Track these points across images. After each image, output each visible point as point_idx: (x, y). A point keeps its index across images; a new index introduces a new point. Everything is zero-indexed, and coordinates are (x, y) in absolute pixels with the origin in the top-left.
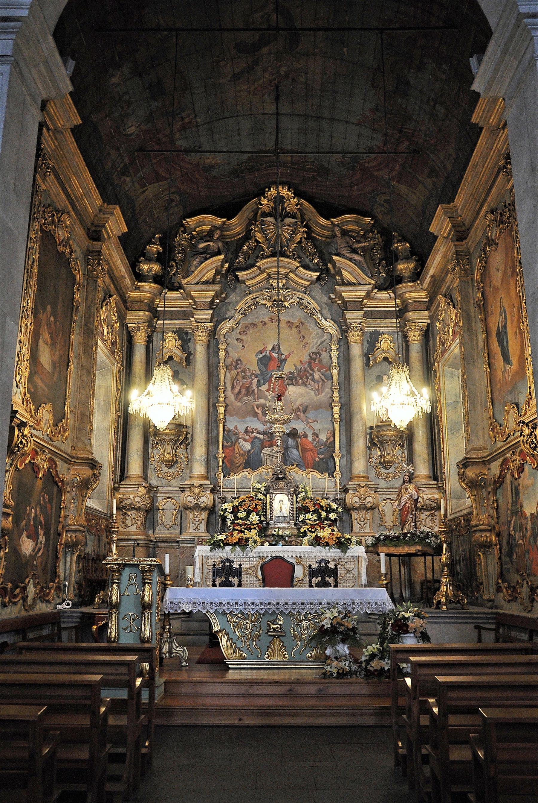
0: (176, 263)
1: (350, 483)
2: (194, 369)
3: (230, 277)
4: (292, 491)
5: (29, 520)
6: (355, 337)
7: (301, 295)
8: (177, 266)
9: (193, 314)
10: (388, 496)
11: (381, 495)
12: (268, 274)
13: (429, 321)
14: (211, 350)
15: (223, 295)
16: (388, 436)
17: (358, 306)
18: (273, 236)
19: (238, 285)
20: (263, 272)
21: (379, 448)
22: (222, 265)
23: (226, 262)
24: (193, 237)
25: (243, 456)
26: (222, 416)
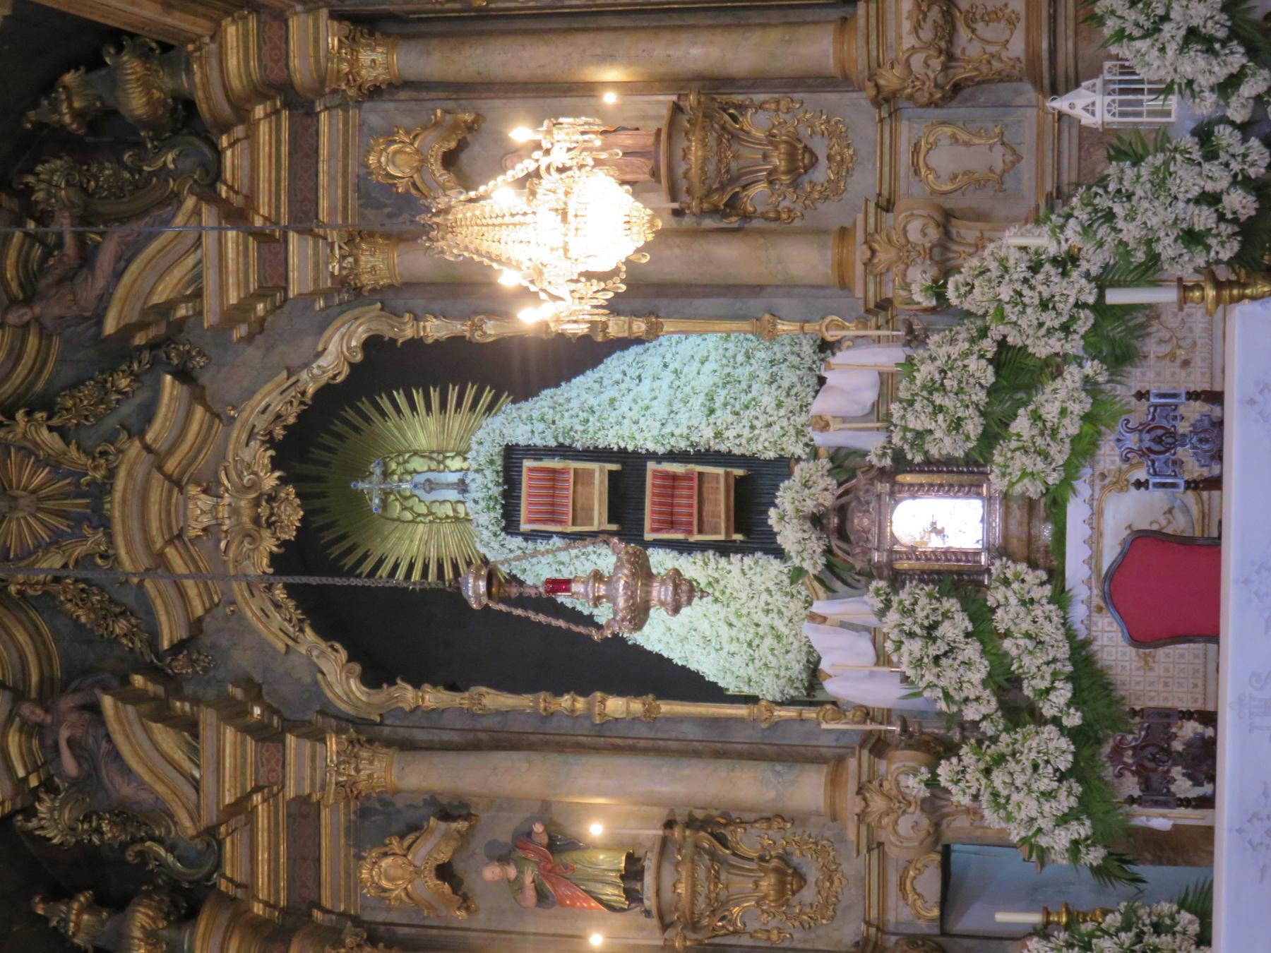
0: (134, 840)
1: (859, 293)
3: (180, 665)
4: (883, 487)
6: (376, 264)
7: (237, 433)
8: (142, 840)
10: (905, 159)
11: (902, 186)
12: (170, 542)
13: (324, 13)
14: (420, 735)
15: (239, 693)
16: (705, 160)
18: (43, 523)
19: (206, 640)
20: (160, 560)
21: (744, 188)
23: (125, 681)
24: (49, 786)
26: (637, 706)
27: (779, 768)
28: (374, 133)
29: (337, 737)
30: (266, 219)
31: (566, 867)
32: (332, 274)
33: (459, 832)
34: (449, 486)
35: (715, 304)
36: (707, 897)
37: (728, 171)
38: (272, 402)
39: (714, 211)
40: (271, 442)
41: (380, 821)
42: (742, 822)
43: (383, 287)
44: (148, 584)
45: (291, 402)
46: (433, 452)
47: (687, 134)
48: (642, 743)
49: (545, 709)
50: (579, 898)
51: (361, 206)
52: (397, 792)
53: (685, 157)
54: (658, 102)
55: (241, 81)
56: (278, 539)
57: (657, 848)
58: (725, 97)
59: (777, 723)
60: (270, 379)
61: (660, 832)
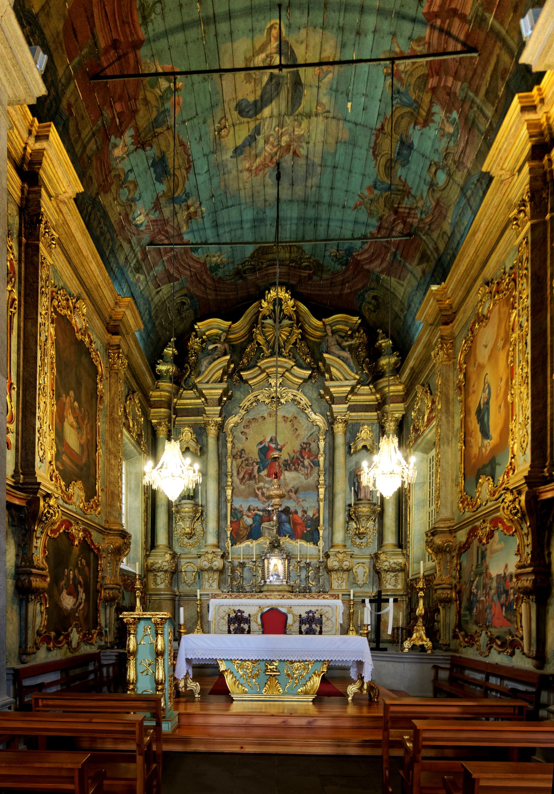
5: (68, 579)
13: (404, 413)
17: (344, 400)
22: (228, 366)
23: (232, 363)
25: (246, 529)
44: (257, 368)
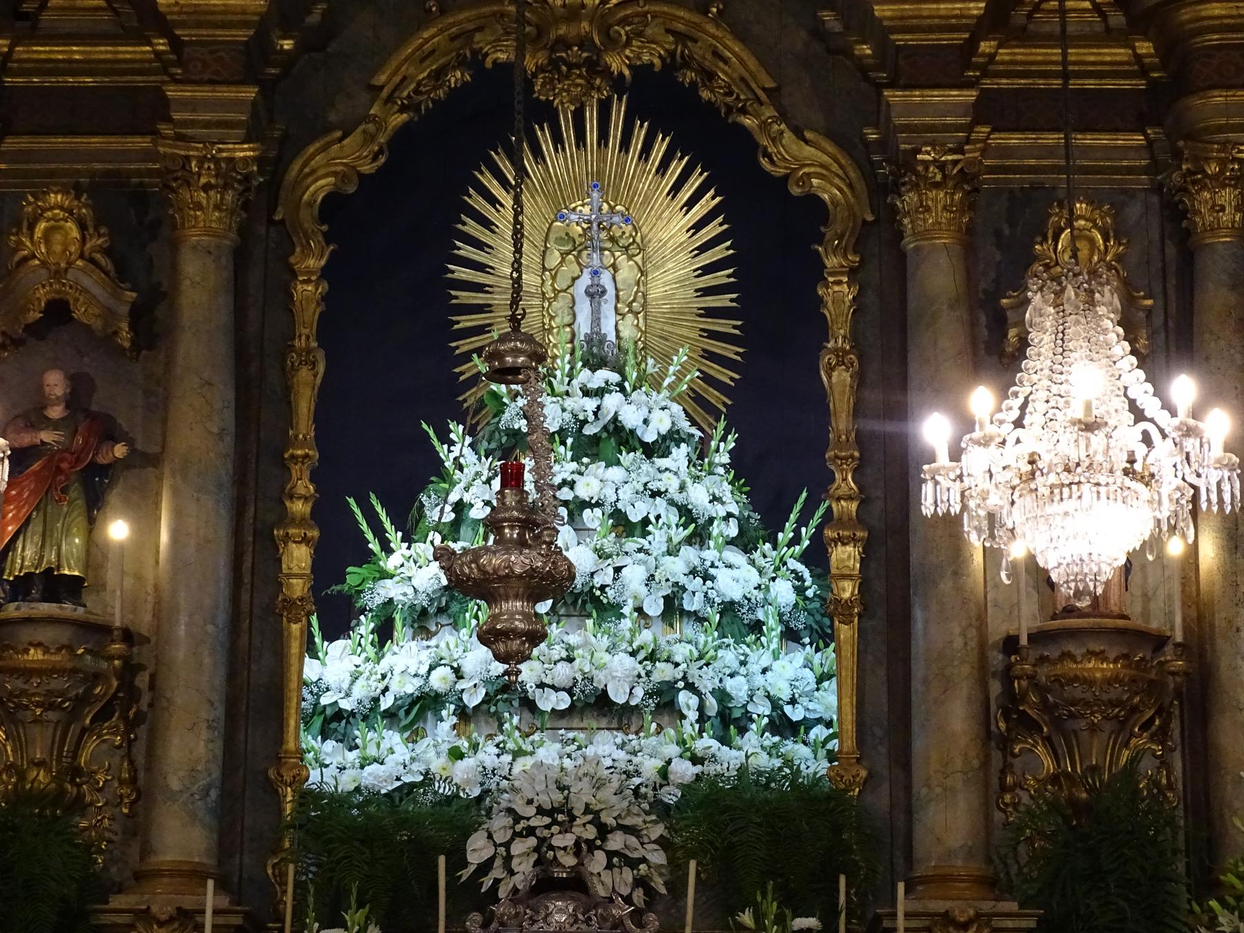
2: (169, 364)
6: (932, 218)
9: (166, 102)
15: (314, 18)
16: (1090, 683)
21: (1048, 740)
27: (214, 794)
28: (1118, 211)
29: (254, 159)
30: (992, 57)
31: (65, 491)
32: (920, 152)
33: (116, 333)
34: (596, 319)
35: (880, 701)
36: (24, 693)
37: (1072, 716)
38: (732, 65)
39: (1011, 700)
40: (672, 64)
41: (133, 222)
42: (130, 742)
43: (900, 223)
45: (730, 93)
46: (644, 296)
47: (1126, 657)
48: (245, 597)
49: (293, 457)
50: (19, 509)
51: (1011, 191)
52: (174, 246)
53: (1091, 654)
54: (1171, 613)
55: (1190, 21)
56: (535, 75)
57: (92, 618)
58: (1177, 712)
59: (277, 791)
60: (762, 63)
61: (118, 624)
